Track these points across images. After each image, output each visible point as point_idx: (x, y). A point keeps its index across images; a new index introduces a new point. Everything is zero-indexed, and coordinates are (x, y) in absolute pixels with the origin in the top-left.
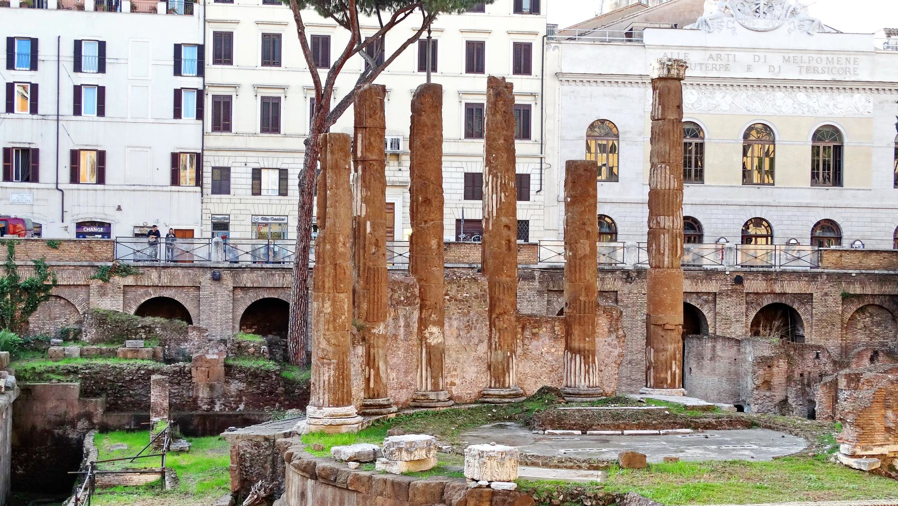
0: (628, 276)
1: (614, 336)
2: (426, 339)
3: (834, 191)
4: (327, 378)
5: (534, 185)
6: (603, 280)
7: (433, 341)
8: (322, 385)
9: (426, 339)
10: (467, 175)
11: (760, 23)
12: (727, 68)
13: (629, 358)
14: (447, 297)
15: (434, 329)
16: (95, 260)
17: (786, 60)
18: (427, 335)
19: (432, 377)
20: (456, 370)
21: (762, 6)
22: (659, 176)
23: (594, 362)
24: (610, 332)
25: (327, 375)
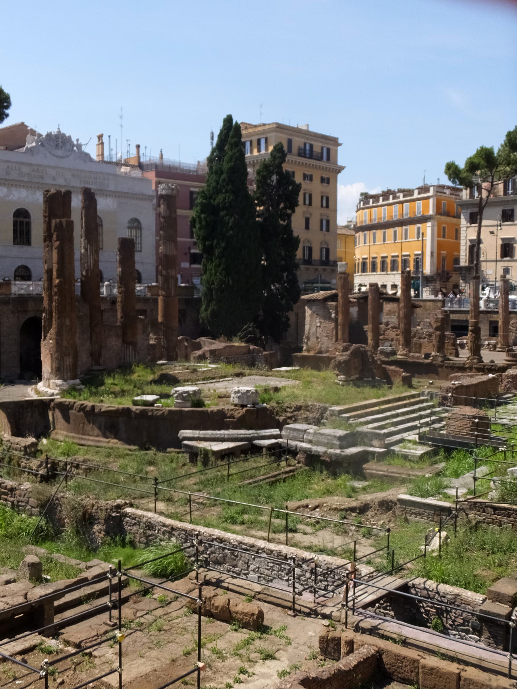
3: (25, 248)
11: (60, 152)
12: (42, 178)
17: (73, 176)
21: (60, 142)
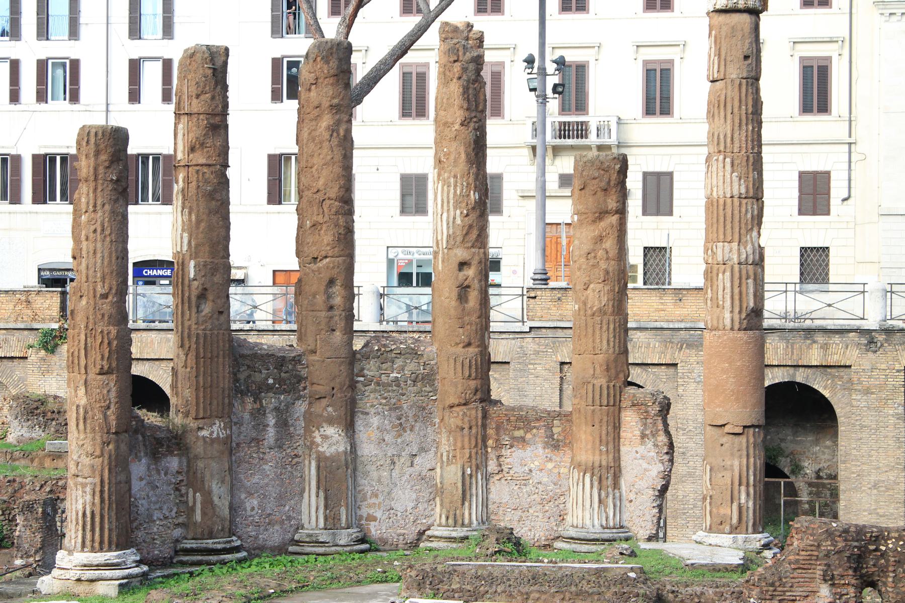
0: (871, 342)
1: (650, 444)
2: (318, 445)
4: (80, 507)
5: (837, 190)
6: (825, 347)
7: (326, 449)
8: (74, 518)
9: (318, 445)
10: (802, 175)
13: (873, 478)
14: (362, 379)
15: (330, 431)
16: (34, 319)
18: (318, 440)
19: (326, 507)
20: (376, 496)
22: (714, 176)
23: (616, 485)
24: (643, 436)
25: (81, 501)
